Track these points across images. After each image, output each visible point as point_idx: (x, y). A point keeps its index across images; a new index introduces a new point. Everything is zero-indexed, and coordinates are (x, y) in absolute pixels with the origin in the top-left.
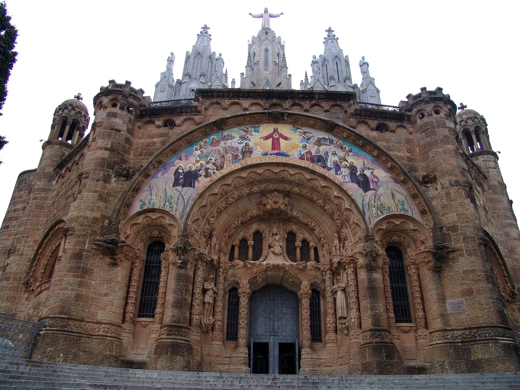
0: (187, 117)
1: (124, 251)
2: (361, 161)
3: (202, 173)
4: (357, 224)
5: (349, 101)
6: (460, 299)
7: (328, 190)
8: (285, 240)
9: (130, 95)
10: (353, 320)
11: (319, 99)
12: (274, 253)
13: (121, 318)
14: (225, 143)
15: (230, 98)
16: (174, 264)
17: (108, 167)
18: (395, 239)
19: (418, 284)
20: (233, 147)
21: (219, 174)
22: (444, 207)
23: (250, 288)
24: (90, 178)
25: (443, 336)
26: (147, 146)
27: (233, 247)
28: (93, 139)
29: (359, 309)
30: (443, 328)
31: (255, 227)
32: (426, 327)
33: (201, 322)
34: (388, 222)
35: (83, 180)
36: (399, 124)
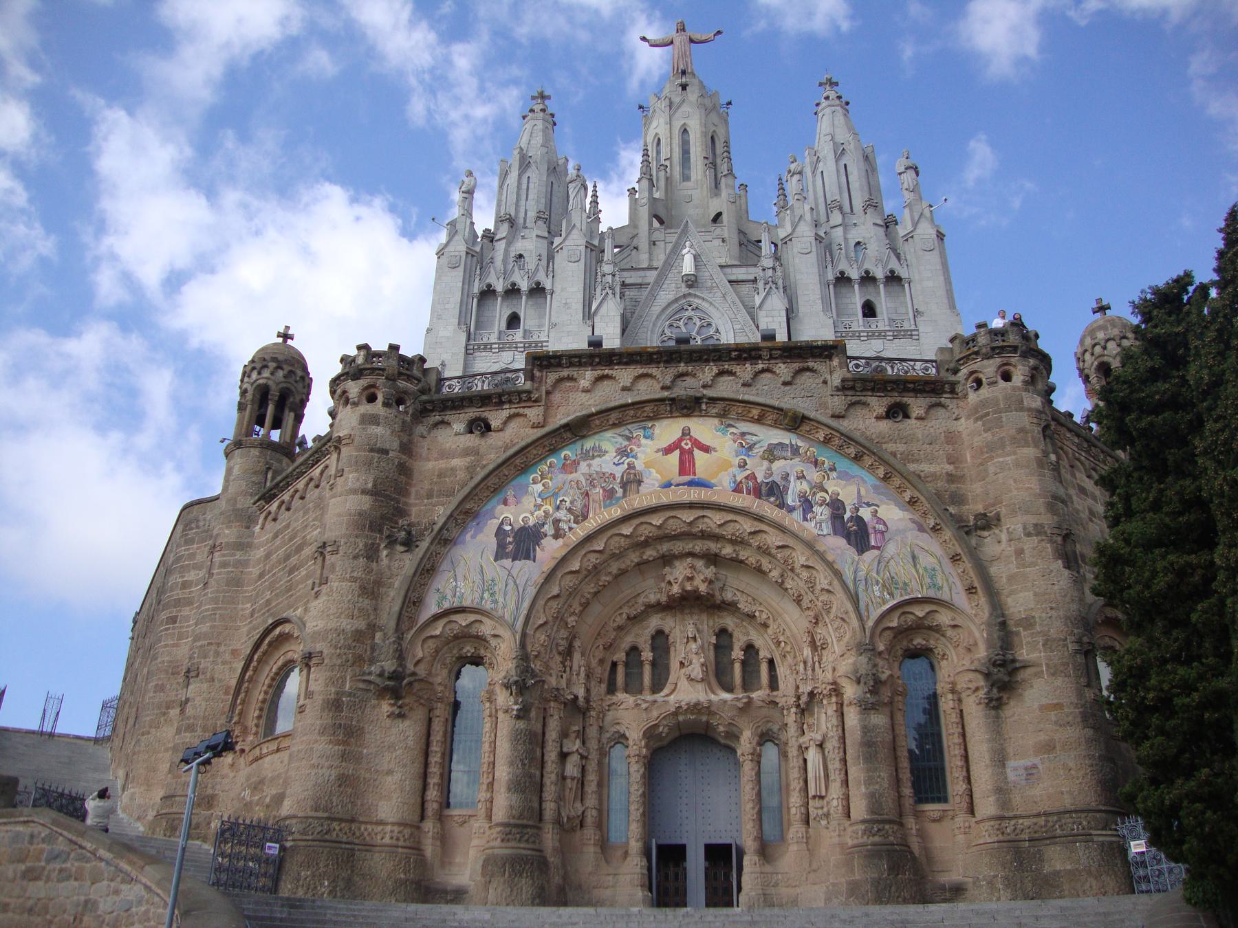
0: (513, 411)
1: (415, 691)
2: (853, 489)
3: (549, 529)
4: (843, 619)
5: (830, 357)
6: (1036, 761)
7: (787, 552)
8: (712, 647)
9: (400, 374)
10: (835, 803)
11: (771, 358)
12: (690, 679)
13: (418, 810)
14: (589, 466)
16: (506, 711)
17: (371, 529)
18: (919, 644)
19: (960, 730)
20: (604, 474)
21: (581, 531)
22: (1011, 578)
23: (646, 746)
24: (341, 553)
25: (998, 829)
26: (439, 476)
27: (614, 665)
28: (337, 471)
29: (846, 782)
30: (1000, 813)
32: (971, 811)
33: (559, 813)
34: (904, 613)
35: (327, 557)
36: (934, 400)
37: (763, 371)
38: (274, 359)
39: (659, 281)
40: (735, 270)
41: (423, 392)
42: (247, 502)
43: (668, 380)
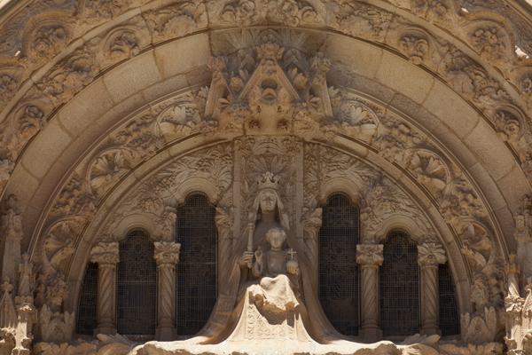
8: (313, 233)
27: (93, 269)
31: (187, 180)
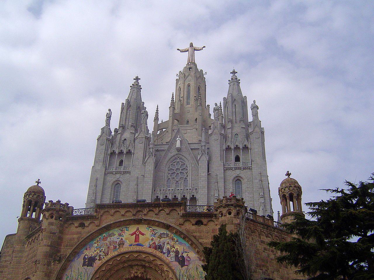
3: (97, 258)
7: (162, 266)
11: (164, 206)
14: (110, 239)
15: (114, 208)
20: (114, 241)
21: (106, 259)
36: (210, 219)
37: (161, 210)
38: (34, 192)
39: (169, 150)
40: (194, 145)
41: (67, 215)
42: (24, 238)
43: (135, 213)
